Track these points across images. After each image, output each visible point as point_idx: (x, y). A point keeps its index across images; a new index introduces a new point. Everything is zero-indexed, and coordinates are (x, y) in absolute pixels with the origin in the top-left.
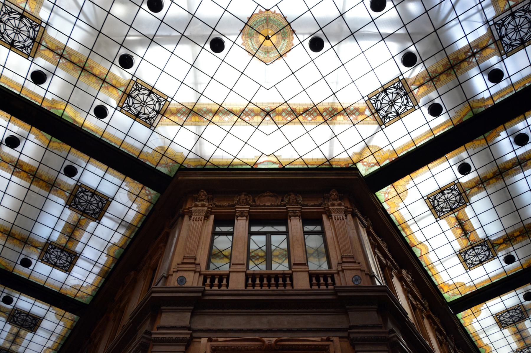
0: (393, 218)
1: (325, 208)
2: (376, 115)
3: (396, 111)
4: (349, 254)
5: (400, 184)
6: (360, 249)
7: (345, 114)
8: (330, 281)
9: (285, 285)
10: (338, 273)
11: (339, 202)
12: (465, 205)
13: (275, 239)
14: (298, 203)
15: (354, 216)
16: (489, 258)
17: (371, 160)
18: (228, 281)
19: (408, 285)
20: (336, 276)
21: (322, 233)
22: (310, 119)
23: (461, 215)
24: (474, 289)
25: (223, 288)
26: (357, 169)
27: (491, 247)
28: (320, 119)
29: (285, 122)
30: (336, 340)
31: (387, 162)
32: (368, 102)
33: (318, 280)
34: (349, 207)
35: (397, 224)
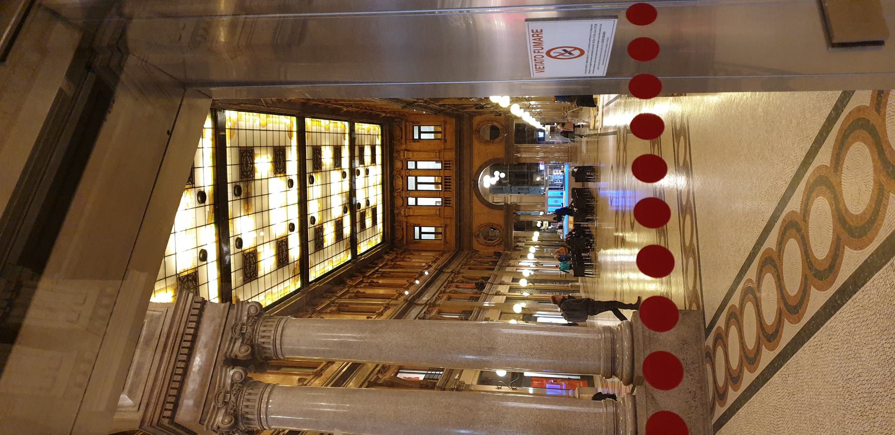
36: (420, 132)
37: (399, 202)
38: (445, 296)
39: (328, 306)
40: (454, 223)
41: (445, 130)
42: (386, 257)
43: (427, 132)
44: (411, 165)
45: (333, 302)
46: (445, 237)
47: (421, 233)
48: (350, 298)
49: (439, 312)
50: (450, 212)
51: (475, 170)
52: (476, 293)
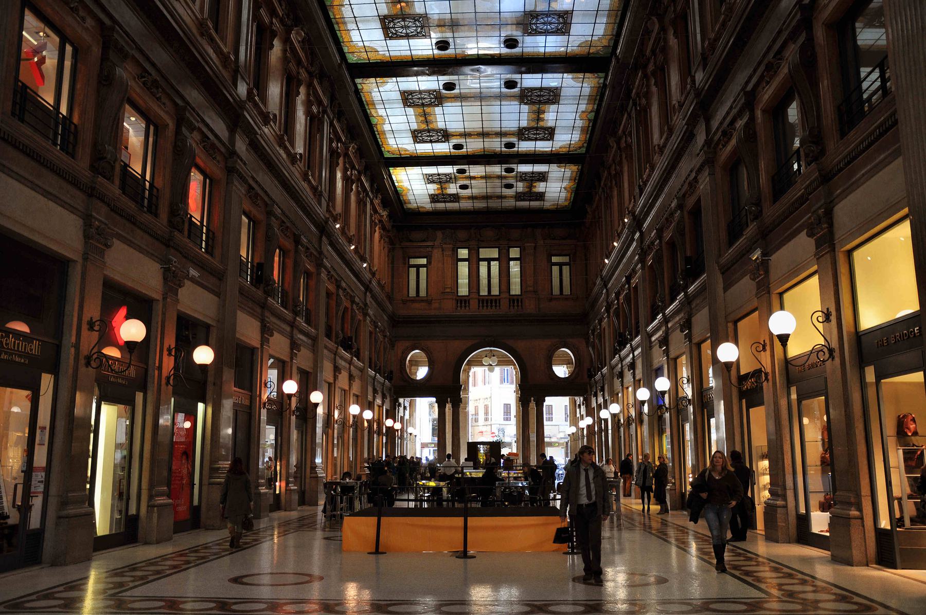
36: (561, 265)
37: (462, 234)
38: (332, 288)
39: (320, 103)
40: (432, 313)
41: (567, 298)
42: (385, 214)
43: (560, 276)
44: (514, 252)
45: (325, 112)
46: (413, 301)
47: (418, 267)
48: (331, 141)
49: (308, 275)
50: (448, 307)
51: (511, 343)
52: (337, 337)
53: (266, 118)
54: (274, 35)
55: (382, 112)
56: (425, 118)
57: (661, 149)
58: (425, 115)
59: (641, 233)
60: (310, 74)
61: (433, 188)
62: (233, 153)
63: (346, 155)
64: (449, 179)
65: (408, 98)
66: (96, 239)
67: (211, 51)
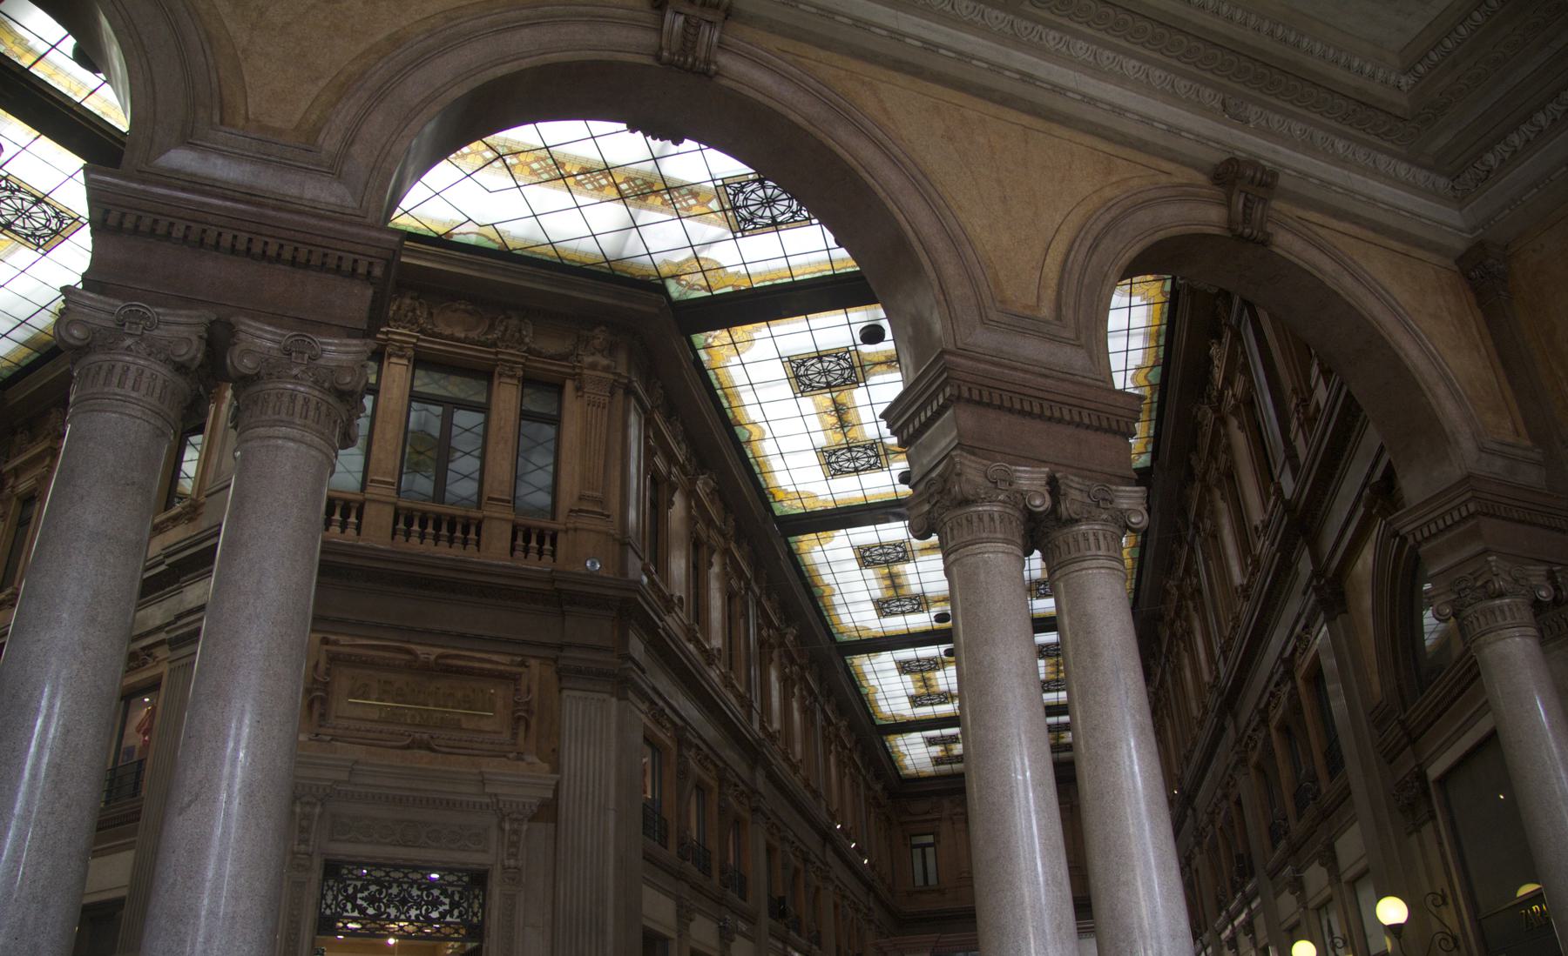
0: (713, 377)
1: (574, 367)
2: (730, 214)
3: (773, 218)
4: (595, 494)
5: (740, 332)
6: (618, 483)
7: (667, 197)
8: (547, 546)
9: (465, 543)
10: (566, 531)
11: (605, 362)
12: (856, 384)
13: (463, 418)
14: (521, 341)
15: (629, 391)
16: (871, 468)
17: (698, 279)
18: (359, 517)
19: (700, 505)
20: (561, 537)
21: (556, 421)
22: (589, 186)
23: (843, 397)
24: (831, 506)
25: (351, 532)
26: (663, 290)
27: (881, 452)
28: (614, 193)
29: (535, 179)
30: (533, 662)
31: (730, 289)
32: (721, 190)
33: (527, 540)
34: (625, 374)
35: (717, 385)
42: (878, 787)
45: (816, 700)
47: (923, 847)
53: (772, 737)
54: (772, 647)
55: (873, 682)
56: (926, 683)
57: (1201, 723)
58: (924, 680)
59: (1194, 810)
60: (802, 668)
61: (936, 750)
62: (755, 792)
63: (837, 736)
64: (953, 739)
65: (904, 667)
66: (684, 916)
67: (731, 697)
